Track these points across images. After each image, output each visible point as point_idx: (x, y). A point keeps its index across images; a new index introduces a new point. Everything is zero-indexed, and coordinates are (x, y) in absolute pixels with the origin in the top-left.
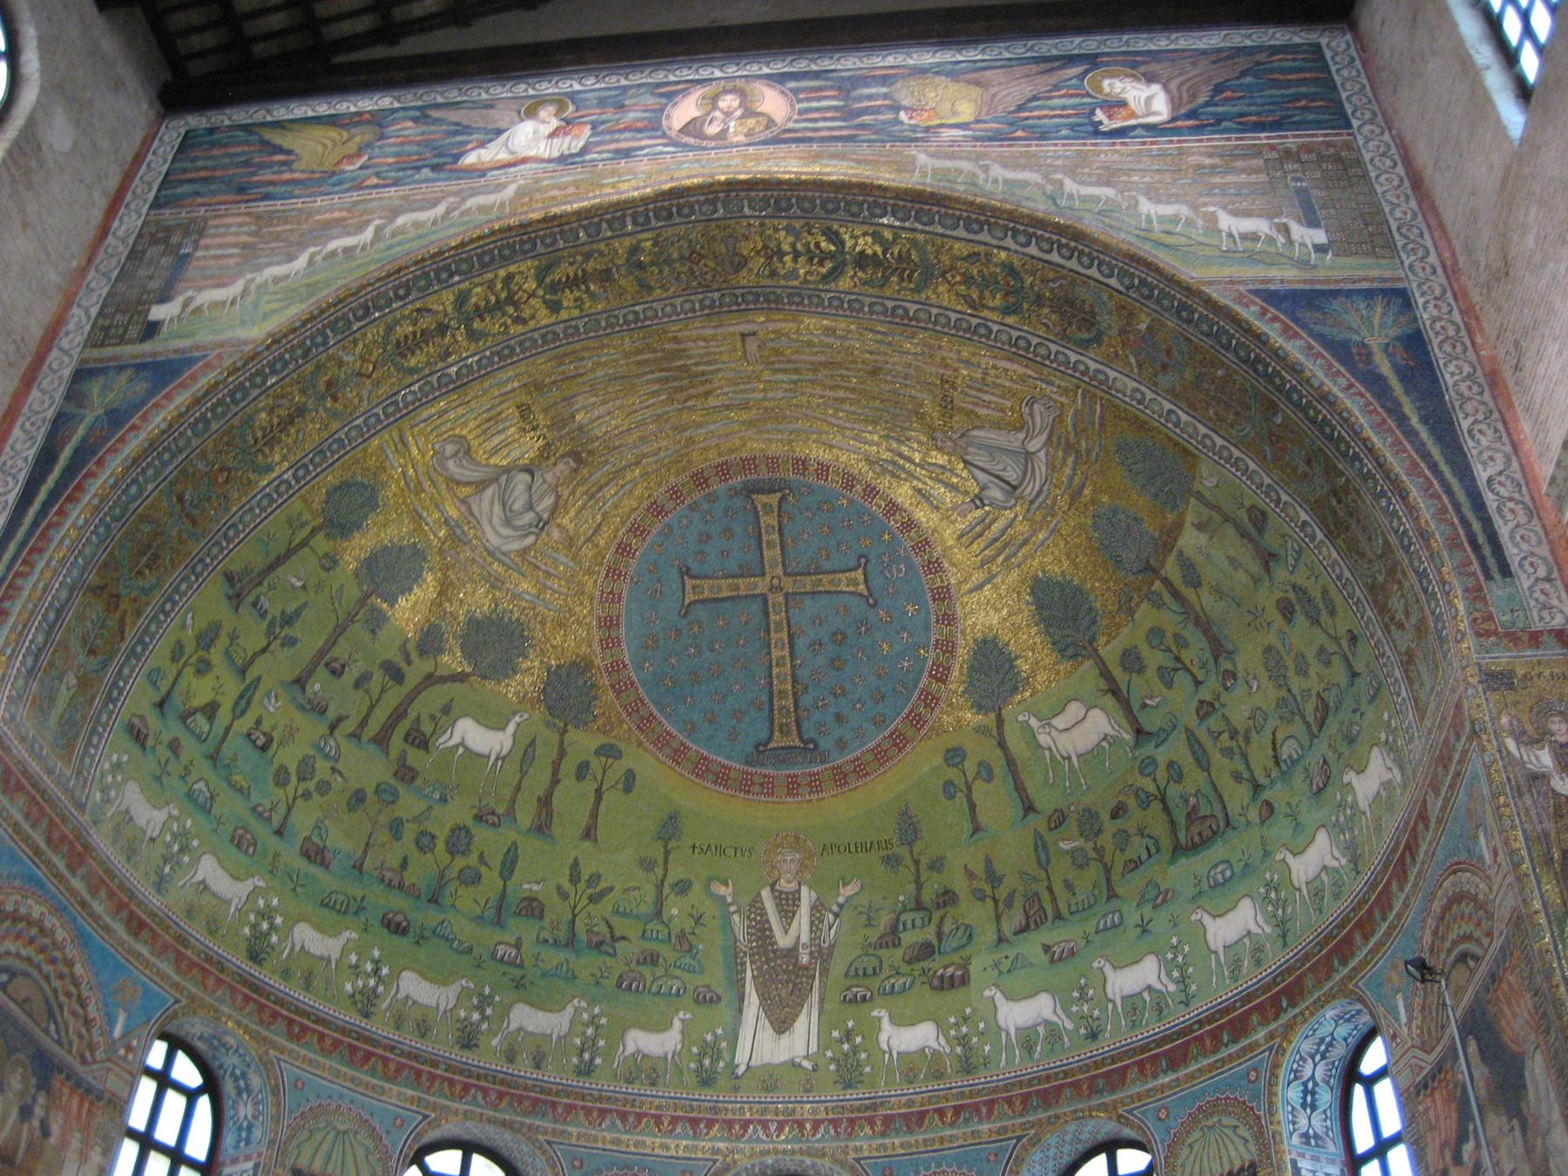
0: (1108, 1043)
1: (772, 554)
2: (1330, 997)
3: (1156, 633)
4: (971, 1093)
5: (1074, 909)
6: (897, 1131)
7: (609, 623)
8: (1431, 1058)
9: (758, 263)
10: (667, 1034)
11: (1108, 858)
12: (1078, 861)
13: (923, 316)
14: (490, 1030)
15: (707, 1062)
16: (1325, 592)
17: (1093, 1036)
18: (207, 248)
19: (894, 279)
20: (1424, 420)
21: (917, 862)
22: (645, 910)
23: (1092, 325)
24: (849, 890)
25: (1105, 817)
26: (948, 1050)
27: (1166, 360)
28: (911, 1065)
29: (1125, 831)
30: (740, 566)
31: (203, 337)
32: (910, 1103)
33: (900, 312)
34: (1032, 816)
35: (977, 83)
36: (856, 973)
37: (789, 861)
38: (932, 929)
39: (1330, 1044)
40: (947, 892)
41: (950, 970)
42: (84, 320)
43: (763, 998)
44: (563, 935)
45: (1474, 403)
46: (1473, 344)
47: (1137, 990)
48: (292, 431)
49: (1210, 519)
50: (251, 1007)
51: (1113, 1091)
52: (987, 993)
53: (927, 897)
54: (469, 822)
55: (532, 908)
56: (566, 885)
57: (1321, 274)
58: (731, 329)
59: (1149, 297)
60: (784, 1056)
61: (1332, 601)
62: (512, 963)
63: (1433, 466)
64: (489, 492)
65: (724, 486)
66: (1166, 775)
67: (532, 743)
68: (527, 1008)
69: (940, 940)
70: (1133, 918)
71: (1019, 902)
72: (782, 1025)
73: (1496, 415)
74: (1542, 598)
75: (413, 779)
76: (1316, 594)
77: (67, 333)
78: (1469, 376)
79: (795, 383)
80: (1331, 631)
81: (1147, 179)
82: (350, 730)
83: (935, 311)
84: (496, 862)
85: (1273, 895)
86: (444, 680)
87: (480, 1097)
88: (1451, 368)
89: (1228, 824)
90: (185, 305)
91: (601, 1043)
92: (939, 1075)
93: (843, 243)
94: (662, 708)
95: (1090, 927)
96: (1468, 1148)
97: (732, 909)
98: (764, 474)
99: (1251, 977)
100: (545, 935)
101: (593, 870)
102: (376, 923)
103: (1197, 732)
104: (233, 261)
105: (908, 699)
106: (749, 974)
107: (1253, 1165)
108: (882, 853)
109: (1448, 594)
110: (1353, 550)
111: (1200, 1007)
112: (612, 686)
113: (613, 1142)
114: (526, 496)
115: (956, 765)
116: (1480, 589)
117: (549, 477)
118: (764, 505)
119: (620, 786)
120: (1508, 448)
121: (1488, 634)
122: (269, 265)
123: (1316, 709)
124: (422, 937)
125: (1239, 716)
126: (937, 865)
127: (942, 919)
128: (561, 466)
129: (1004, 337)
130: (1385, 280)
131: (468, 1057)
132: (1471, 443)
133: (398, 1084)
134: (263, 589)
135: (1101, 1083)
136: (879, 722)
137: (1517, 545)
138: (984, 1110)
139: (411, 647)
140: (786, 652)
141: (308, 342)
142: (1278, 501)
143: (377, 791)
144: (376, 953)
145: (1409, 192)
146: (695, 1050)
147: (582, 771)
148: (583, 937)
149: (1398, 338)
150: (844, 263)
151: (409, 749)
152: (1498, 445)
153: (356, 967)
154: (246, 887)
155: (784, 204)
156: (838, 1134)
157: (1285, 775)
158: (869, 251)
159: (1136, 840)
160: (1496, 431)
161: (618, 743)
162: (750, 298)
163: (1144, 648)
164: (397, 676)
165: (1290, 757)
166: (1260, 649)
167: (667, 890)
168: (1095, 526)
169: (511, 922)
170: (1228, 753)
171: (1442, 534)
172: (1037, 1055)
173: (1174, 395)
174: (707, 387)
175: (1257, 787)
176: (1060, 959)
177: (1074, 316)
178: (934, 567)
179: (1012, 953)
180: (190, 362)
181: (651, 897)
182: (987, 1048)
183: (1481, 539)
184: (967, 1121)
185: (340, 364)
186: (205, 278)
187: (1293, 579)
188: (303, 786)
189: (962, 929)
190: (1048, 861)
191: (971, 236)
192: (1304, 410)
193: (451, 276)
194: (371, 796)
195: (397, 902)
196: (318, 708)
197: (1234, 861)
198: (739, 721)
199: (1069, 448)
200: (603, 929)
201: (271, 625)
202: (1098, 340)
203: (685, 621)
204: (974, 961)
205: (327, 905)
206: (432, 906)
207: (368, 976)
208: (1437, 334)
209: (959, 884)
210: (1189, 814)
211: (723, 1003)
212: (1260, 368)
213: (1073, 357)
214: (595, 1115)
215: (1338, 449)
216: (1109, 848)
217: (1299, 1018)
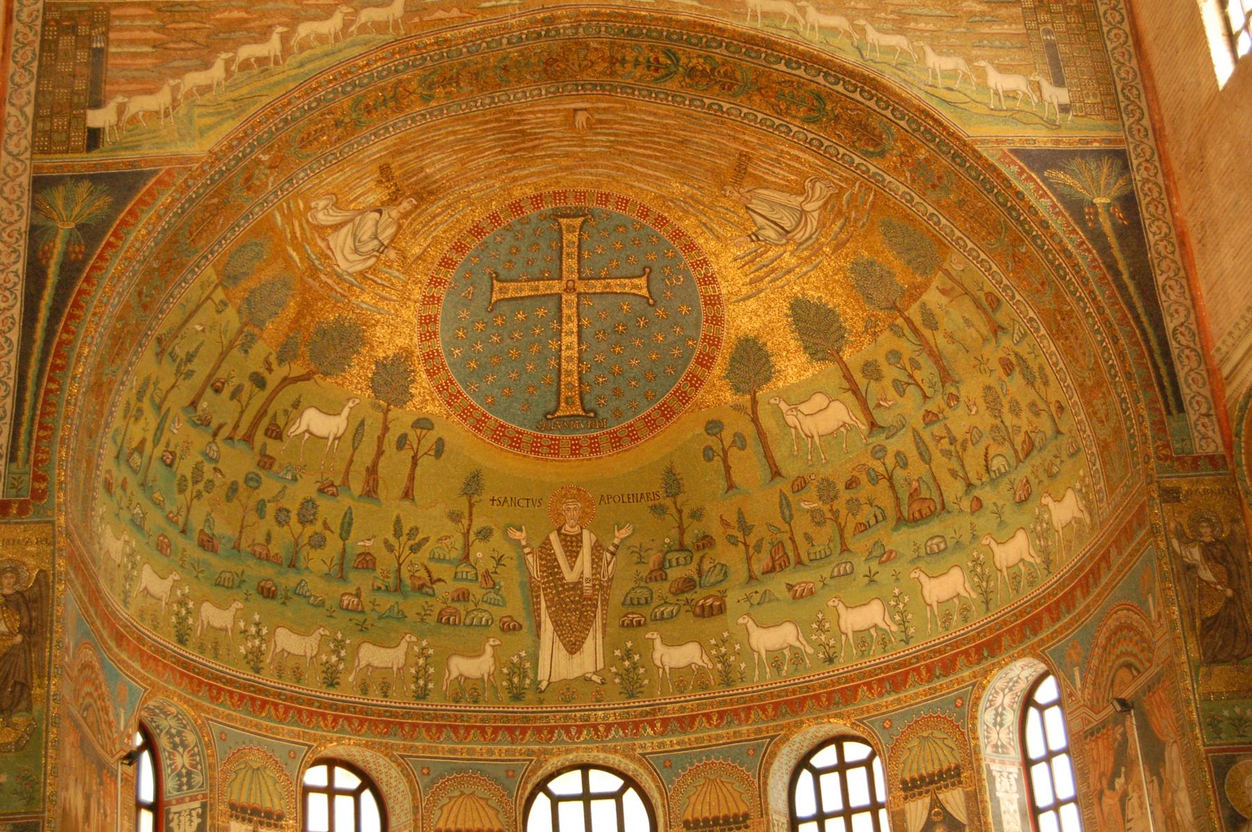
0: (844, 664)
1: (570, 263)
2: (1021, 655)
3: (894, 356)
4: (731, 701)
5: (812, 557)
6: (673, 733)
7: (426, 321)
8: (1098, 717)
10: (482, 659)
12: (818, 519)
13: (733, 111)
14: (346, 668)
15: (516, 680)
17: (830, 660)
18: (120, 42)
20: (1132, 277)
21: (680, 512)
22: (454, 555)
23: (878, 144)
24: (624, 533)
25: (841, 486)
26: (710, 666)
27: (936, 182)
28: (683, 678)
30: (542, 272)
31: (148, 151)
32: (683, 709)
34: (778, 479)
36: (631, 603)
37: (572, 509)
38: (693, 567)
39: (1017, 682)
40: (705, 537)
41: (710, 601)
42: (23, 122)
43: (557, 624)
44: (391, 582)
45: (1168, 261)
46: (1170, 204)
47: (866, 627)
49: (953, 289)
50: (186, 680)
51: (847, 703)
52: (741, 621)
53: (688, 540)
54: (314, 495)
55: (367, 562)
56: (392, 540)
57: (1064, 133)
58: (567, 106)
60: (577, 673)
62: (355, 611)
63: (1137, 318)
64: (345, 230)
67: (362, 423)
68: (371, 646)
69: (700, 577)
70: (862, 568)
71: (766, 547)
72: (573, 648)
73: (1182, 273)
74: (1203, 430)
75: (271, 465)
77: (11, 135)
78: (1166, 235)
80: (1043, 395)
81: (931, 26)
82: (227, 434)
84: (336, 525)
85: (979, 570)
86: (296, 380)
87: (346, 726)
88: (1154, 229)
89: (943, 508)
90: (121, 110)
91: (431, 670)
96: (1120, 782)
97: (527, 550)
98: (572, 203)
99: (958, 628)
100: (379, 583)
101: (412, 525)
102: (253, 592)
103: (921, 432)
104: (149, 62)
105: (677, 379)
107: (957, 767)
108: (651, 503)
109: (1141, 424)
111: (916, 646)
112: (427, 371)
113: (450, 751)
114: (374, 228)
116: (1162, 422)
117: (394, 214)
118: (568, 226)
119: (432, 452)
120: (1188, 303)
121: (1166, 458)
122: (188, 70)
123: (1024, 442)
124: (287, 598)
125: (959, 431)
126: (697, 515)
127: (702, 557)
130: (1110, 141)
131: (334, 694)
132: (1163, 297)
133: (288, 724)
134: (177, 341)
135: (837, 697)
136: (650, 398)
137: (1189, 386)
138: (743, 715)
139: (273, 359)
140: (575, 339)
142: (1013, 297)
143: (247, 480)
144: (257, 617)
145: (1132, 50)
146: (505, 671)
147: (402, 442)
148: (408, 582)
149: (1118, 199)
150: (675, 73)
151: (270, 442)
152: (1182, 300)
153: (246, 631)
154: (168, 583)
156: (626, 735)
159: (866, 508)
160: (1182, 287)
163: (882, 361)
164: (259, 382)
165: (998, 469)
167: (472, 537)
168: (853, 270)
169: (352, 575)
170: (946, 453)
171: (1140, 376)
172: (784, 673)
173: (938, 205)
174: (536, 142)
175: (970, 485)
176: (801, 596)
177: (863, 135)
178: (709, 280)
179: (761, 589)
180: (143, 176)
181: (459, 544)
182: (743, 666)
183: (1166, 383)
184: (729, 723)
185: (258, 162)
186: (131, 80)
187: (1016, 349)
189: (719, 567)
190: (791, 516)
192: (1046, 253)
193: (353, 89)
194: (242, 485)
196: (205, 422)
197: (948, 538)
200: (423, 574)
201: (179, 366)
202: (882, 154)
203: (492, 315)
204: (729, 594)
205: (218, 585)
206: (293, 570)
207: (254, 637)
208: (1146, 195)
209: (716, 530)
210: (911, 494)
211: (524, 630)
212: (1014, 214)
213: (857, 160)
214: (434, 730)
215: (1068, 287)
216: (843, 512)
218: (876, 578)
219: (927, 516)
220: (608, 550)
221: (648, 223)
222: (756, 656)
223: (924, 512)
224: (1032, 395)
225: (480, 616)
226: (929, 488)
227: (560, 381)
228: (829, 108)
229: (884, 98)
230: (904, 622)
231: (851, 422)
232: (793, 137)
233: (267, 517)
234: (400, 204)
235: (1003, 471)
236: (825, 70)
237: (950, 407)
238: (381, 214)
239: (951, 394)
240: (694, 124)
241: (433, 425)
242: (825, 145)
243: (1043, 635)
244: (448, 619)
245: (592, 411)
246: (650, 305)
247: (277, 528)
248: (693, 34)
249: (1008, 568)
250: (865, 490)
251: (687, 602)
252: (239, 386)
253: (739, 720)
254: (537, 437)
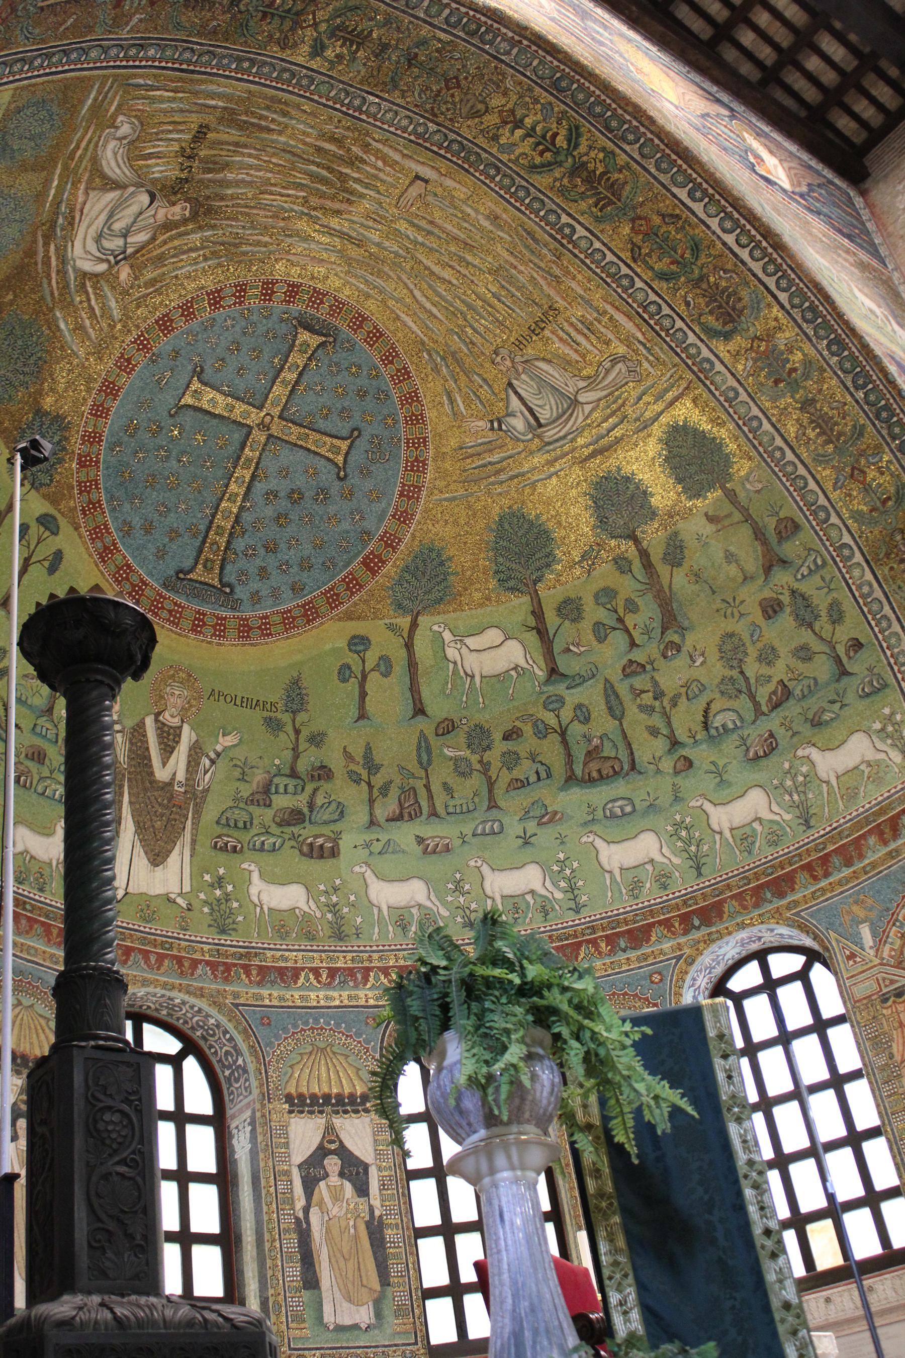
3: (606, 595)
5: (451, 810)
6: (273, 983)
9: (492, 119)
10: (51, 840)
11: (493, 773)
13: (583, 244)
21: (297, 732)
23: (733, 321)
25: (497, 736)
26: (319, 915)
34: (420, 718)
35: (665, 73)
41: (320, 841)
43: (140, 828)
52: (357, 869)
53: (302, 766)
60: (157, 889)
65: (284, 306)
66: (572, 714)
69: (311, 812)
70: (514, 828)
72: (157, 858)
79: (415, 242)
83: (597, 245)
89: (633, 766)
92: (310, 936)
93: (576, 146)
94: (112, 498)
95: (468, 830)
99: (650, 895)
103: (616, 685)
105: (333, 577)
108: (266, 714)
114: (132, 220)
115: (358, 652)
119: (46, 564)
123: (774, 693)
126: (317, 740)
127: (316, 790)
128: (177, 209)
129: (640, 296)
136: (297, 589)
138: (359, 976)
140: (242, 491)
150: (560, 164)
155: (564, 84)
156: (216, 977)
158: (591, 166)
159: (526, 764)
161: (59, 516)
162: (455, 147)
166: (720, 633)
170: (648, 710)
175: (675, 744)
179: (384, 838)
182: (359, 920)
187: (796, 586)
189: (334, 805)
190: (430, 762)
197: (637, 802)
198: (171, 540)
202: (727, 336)
204: (343, 836)
209: (336, 763)
210: (589, 753)
213: (692, 338)
216: (496, 764)
217: (715, 936)
218: (532, 840)
219: (608, 777)
220: (208, 756)
221: (386, 372)
222: (376, 911)
223: (604, 772)
224: (806, 636)
225: (53, 787)
226: (615, 746)
227: (206, 536)
229: (779, 261)
230: (572, 889)
231: (525, 666)
234: (174, 204)
235: (731, 726)
236: (730, 209)
237: (665, 657)
238: (151, 203)
239: (672, 642)
241: (58, 528)
242: (663, 313)
243: (789, 898)
245: (229, 585)
246: (340, 479)
248: (620, 111)
249: (731, 829)
250: (528, 742)
251: (293, 837)
253: (355, 980)
254: (161, 596)
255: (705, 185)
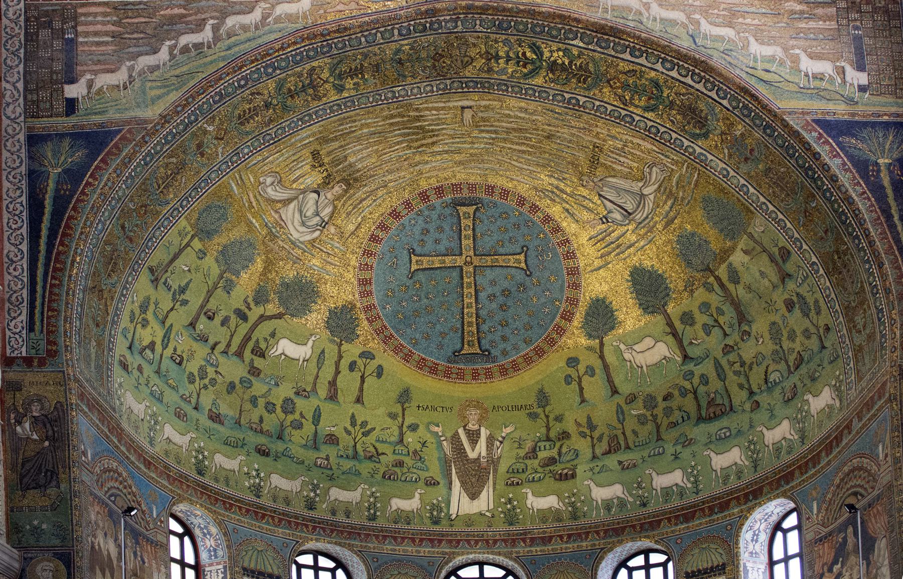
5: (637, 444)
13: (589, 105)
16: (816, 301)
19: (574, 80)
29: (671, 408)
33: (574, 101)
36: (511, 471)
41: (566, 471)
43: (463, 484)
44: (350, 452)
48: (179, 177)
52: (586, 483)
59: (748, 116)
61: (819, 307)
62: (326, 468)
72: (474, 496)
76: (810, 301)
83: (597, 103)
89: (731, 409)
95: (646, 454)
100: (341, 453)
106: (454, 471)
110: (840, 285)
129: (642, 125)
134: (168, 274)
141: (186, 121)
148: (362, 454)
157: (770, 390)
170: (736, 373)
175: (752, 393)
176: (628, 468)
177: (692, 118)
179: (600, 464)
187: (798, 290)
188: (203, 382)
191: (633, 59)
192: (832, 203)
194: (238, 386)
195: (262, 440)
199: (670, 195)
201: (174, 294)
202: (706, 136)
204: (578, 467)
211: (441, 485)
212: (810, 173)
225: (411, 475)
226: (722, 397)
228: (665, 95)
232: (635, 126)
233: (259, 406)
236: (663, 56)
240: (557, 119)
242: (661, 131)
244: (390, 477)
247: (267, 414)
252: (226, 317)
255: (638, 47)
